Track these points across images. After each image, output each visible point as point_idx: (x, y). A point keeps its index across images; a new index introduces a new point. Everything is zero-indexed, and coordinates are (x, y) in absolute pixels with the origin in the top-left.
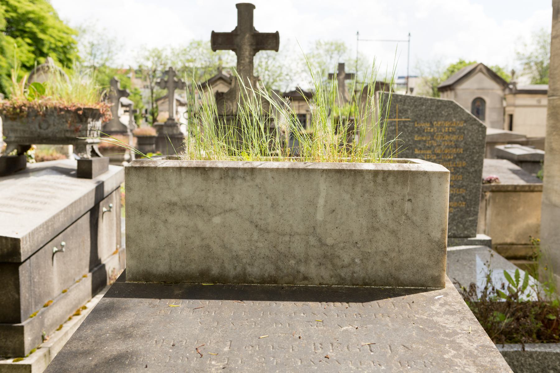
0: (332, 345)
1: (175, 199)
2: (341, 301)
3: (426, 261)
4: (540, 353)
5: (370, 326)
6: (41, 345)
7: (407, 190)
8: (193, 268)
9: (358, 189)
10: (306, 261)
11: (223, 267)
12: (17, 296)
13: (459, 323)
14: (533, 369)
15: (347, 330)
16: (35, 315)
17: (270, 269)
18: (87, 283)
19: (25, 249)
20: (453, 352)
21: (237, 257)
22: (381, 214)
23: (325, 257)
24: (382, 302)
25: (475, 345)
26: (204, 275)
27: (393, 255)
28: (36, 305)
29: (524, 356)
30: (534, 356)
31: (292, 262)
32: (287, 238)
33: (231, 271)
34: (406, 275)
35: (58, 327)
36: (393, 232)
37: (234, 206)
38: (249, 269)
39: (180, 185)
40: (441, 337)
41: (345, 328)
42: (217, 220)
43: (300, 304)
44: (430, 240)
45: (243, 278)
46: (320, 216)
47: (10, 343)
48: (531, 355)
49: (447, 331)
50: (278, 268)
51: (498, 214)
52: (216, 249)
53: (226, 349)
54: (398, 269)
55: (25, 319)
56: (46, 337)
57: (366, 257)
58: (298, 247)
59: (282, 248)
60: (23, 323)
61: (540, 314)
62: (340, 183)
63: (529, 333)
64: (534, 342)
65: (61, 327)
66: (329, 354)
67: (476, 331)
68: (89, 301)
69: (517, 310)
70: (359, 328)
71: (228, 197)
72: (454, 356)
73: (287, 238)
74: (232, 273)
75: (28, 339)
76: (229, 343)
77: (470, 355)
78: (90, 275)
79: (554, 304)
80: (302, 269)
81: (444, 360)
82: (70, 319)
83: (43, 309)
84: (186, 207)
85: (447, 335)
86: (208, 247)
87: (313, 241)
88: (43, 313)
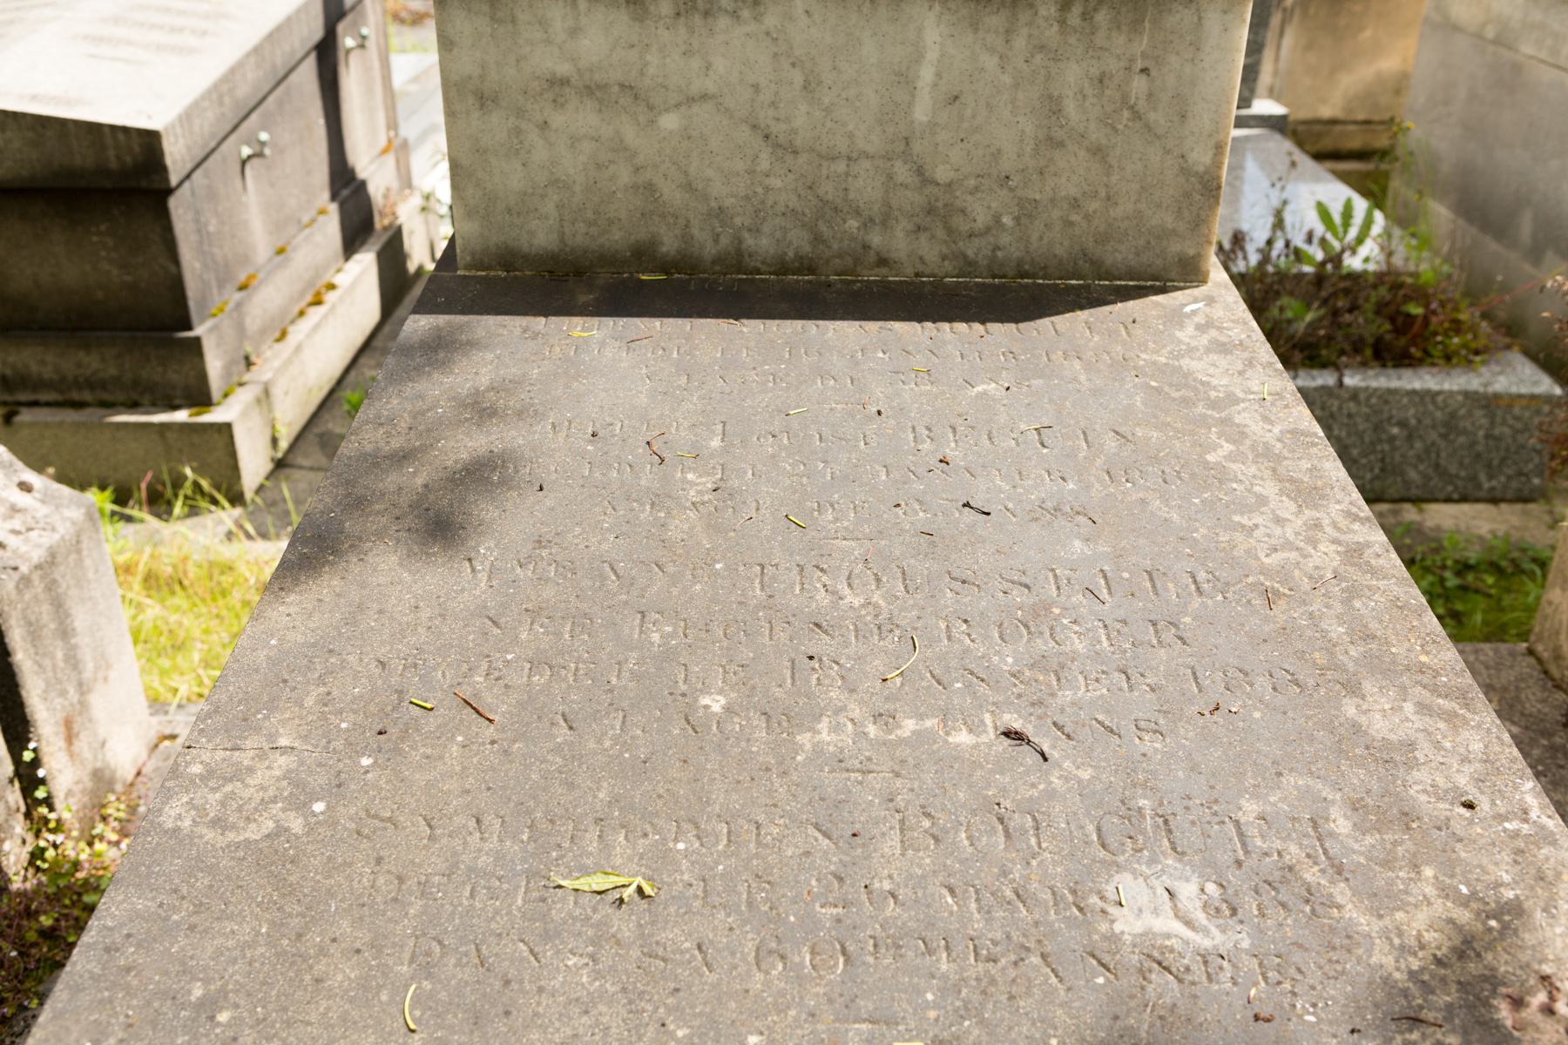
0: (954, 430)
1: (564, 69)
2: (967, 319)
3: (1169, 220)
4: (1376, 390)
5: (1037, 382)
6: (246, 377)
7: (1143, 43)
8: (617, 239)
9: (1020, 42)
10: (886, 220)
11: (686, 237)
12: (173, 269)
13: (1241, 373)
14: (1355, 425)
15: (985, 393)
16: (222, 310)
17: (798, 241)
18: (331, 228)
19: (176, 155)
20: (1228, 447)
21: (720, 213)
22: (1070, 107)
23: (930, 211)
24: (1063, 321)
25: (1276, 430)
26: (643, 254)
27: (1093, 206)
28: (221, 286)
29: (1338, 397)
30: (1362, 396)
31: (853, 224)
32: (841, 167)
33: (707, 243)
34: (1119, 254)
35: (277, 334)
36: (1098, 152)
37: (710, 85)
38: (749, 241)
39: (574, 32)
40: (1200, 409)
41: (980, 388)
42: (670, 122)
43: (873, 326)
44: (1185, 171)
45: (736, 261)
46: (921, 113)
47: (176, 375)
48: (1355, 394)
49: (1213, 394)
50: (817, 239)
51: (1309, 47)
52: (671, 193)
53: (716, 443)
54: (1102, 239)
55: (203, 320)
56: (253, 358)
57: (1027, 211)
58: (866, 188)
59: (828, 189)
60: (198, 331)
61: (1387, 304)
62: (975, 27)
63: (1357, 347)
64: (1364, 364)
65: (283, 335)
66: (950, 454)
67: (1279, 395)
68: (339, 271)
69: (1334, 295)
70: (1013, 389)
71: (696, 63)
72: (1229, 457)
73: (841, 167)
74: (710, 250)
75: (214, 365)
76: (720, 427)
77: (1264, 453)
78: (333, 208)
79: (1422, 280)
80: (876, 239)
81: (1207, 466)
82: (302, 313)
83: (238, 296)
84: (593, 91)
85: (1214, 405)
86: (650, 187)
87: (902, 172)
88: (239, 305)
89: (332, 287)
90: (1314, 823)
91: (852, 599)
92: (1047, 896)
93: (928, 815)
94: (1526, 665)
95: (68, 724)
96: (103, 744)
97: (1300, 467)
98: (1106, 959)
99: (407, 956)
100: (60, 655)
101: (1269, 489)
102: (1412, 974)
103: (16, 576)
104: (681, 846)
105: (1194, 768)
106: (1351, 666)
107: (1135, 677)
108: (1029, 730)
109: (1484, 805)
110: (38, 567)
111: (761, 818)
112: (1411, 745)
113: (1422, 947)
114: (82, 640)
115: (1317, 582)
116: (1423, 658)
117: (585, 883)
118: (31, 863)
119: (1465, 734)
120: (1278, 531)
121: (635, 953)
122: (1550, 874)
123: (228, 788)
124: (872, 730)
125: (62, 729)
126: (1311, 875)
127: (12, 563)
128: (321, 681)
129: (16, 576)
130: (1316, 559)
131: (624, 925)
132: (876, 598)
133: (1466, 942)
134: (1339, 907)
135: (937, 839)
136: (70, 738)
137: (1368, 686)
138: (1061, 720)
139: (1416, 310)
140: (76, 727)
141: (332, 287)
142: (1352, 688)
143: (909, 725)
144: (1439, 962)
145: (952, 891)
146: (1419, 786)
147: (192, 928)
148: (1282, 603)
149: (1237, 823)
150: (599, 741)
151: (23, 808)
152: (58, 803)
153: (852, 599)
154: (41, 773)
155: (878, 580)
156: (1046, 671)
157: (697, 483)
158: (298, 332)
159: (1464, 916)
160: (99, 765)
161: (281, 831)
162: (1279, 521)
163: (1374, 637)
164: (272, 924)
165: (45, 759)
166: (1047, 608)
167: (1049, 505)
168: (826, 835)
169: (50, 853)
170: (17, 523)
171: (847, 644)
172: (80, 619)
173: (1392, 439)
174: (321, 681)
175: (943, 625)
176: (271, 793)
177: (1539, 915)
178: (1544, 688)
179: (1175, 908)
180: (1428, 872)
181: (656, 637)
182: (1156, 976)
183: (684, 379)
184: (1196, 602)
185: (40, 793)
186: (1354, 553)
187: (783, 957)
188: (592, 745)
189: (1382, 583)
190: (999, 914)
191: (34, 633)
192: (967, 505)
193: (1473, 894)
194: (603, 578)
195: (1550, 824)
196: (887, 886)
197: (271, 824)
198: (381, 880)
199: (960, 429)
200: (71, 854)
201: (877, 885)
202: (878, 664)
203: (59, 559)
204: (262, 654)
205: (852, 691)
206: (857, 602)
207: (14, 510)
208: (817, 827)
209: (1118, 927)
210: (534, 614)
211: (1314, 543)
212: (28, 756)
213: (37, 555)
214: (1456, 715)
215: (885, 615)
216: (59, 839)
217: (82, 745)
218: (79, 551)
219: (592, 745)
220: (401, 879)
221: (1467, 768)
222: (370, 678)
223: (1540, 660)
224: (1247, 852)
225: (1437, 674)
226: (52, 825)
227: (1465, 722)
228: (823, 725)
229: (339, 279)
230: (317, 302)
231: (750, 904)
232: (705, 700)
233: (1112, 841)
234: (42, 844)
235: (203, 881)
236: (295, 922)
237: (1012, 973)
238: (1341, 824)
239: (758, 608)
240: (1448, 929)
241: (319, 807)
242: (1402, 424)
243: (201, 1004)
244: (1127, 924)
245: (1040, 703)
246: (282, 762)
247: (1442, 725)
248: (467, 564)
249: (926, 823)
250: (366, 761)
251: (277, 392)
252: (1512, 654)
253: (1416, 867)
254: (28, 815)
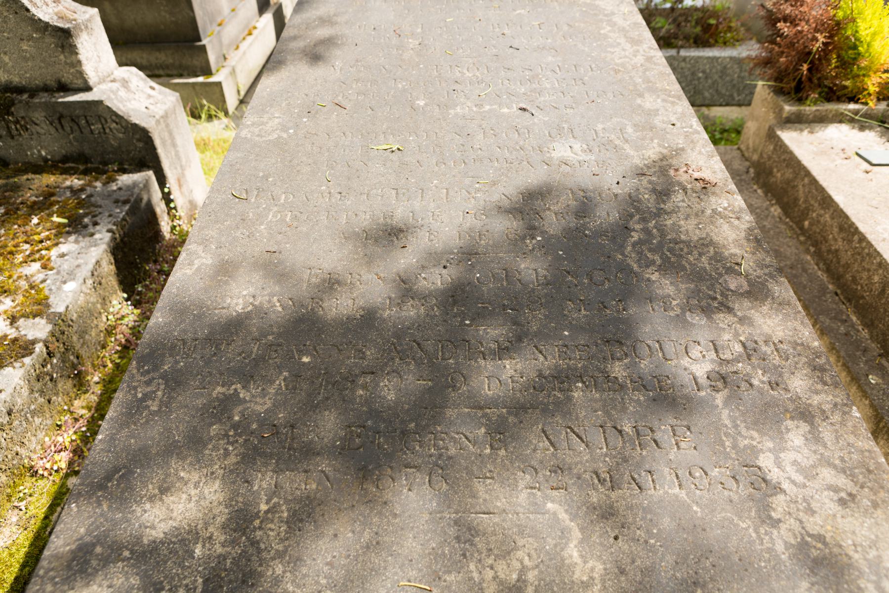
0: (508, 25)
4: (693, 57)
5: (540, 10)
6: (225, 64)
12: (191, 14)
13: (618, 5)
14: (684, 73)
15: (520, 14)
16: (212, 34)
20: (609, 28)
25: (628, 23)
28: (211, 23)
29: (677, 60)
30: (688, 60)
35: (235, 47)
40: (601, 17)
41: (518, 12)
47: (197, 62)
48: (684, 59)
49: (606, 12)
53: (419, 30)
55: (205, 38)
56: (227, 56)
60: (204, 42)
61: (702, 18)
63: (686, 38)
64: (690, 47)
65: (237, 48)
66: (505, 32)
67: (631, 12)
68: (257, 21)
69: (680, 15)
70: (531, 12)
72: (609, 31)
76: (420, 26)
77: (623, 30)
79: (716, 8)
81: (600, 34)
82: (244, 39)
83: (218, 28)
85: (606, 15)
88: (219, 32)
89: (255, 28)
90: (621, 130)
91: (468, 74)
92: (531, 148)
93: (492, 130)
94: (736, 153)
95: (179, 181)
96: (192, 191)
97: (635, 34)
98: (548, 162)
99: (325, 165)
100: (173, 153)
101: (622, 40)
102: (645, 165)
103: (155, 119)
104: (411, 138)
105: (583, 117)
106: (642, 90)
107: (566, 94)
108: (528, 108)
109: (678, 125)
110: (162, 117)
111: (437, 131)
112: (658, 110)
113: (649, 158)
114: (180, 149)
115: (634, 67)
116: (668, 87)
117: (380, 147)
118: (172, 232)
119: (677, 107)
120: (623, 53)
121: (398, 163)
122: (695, 141)
123: (261, 127)
124: (475, 109)
125: (177, 182)
126: (617, 142)
127: (153, 115)
128: (286, 99)
129: (155, 119)
130: (635, 60)
131: (394, 157)
132: (478, 74)
133: (664, 157)
134: (625, 150)
135: (495, 136)
136: (180, 186)
137: (646, 95)
138: (539, 105)
139: (713, 21)
140: (182, 183)
141: (255, 28)
142: (641, 95)
143: (487, 108)
144: (654, 162)
145: (499, 148)
146: (657, 121)
147: (256, 160)
148: (621, 73)
149: (595, 131)
150: (383, 113)
151: (166, 211)
152: (179, 209)
153: (468, 74)
154: (172, 197)
155: (478, 69)
156: (535, 93)
157: (412, 43)
158: (244, 46)
159: (665, 151)
160: (191, 198)
161: (279, 137)
162: (624, 50)
163: (651, 82)
164: (281, 159)
165: (173, 192)
166: (537, 75)
167: (541, 46)
168: (459, 135)
169: (178, 228)
170: (151, 101)
171: (466, 87)
172: (179, 141)
173: (699, 79)
174: (286, 99)
175: (500, 81)
176: (275, 128)
177: (689, 151)
178: (741, 160)
179: (572, 151)
180: (656, 141)
181: (400, 86)
182: (563, 166)
183: (406, 11)
184: (590, 73)
185: (172, 205)
186: (649, 59)
187: (445, 164)
188: (380, 114)
189: (657, 67)
190: (514, 153)
191: (164, 143)
192: (511, 47)
193: (669, 146)
194: (381, 70)
195: (699, 129)
196: (478, 147)
197: (277, 136)
198: (314, 148)
199: (510, 25)
200: (186, 229)
201: (475, 146)
202: (477, 92)
203: (169, 115)
204: (265, 93)
205: (468, 99)
206: (470, 75)
207: (150, 96)
208: (456, 133)
209: (552, 155)
210: (357, 81)
211: (635, 56)
212: (166, 190)
213: (161, 113)
214: (675, 102)
215: (480, 78)
216: (181, 223)
217: (184, 189)
218: (175, 114)
219: (380, 114)
220: (321, 148)
221: (675, 116)
222: (303, 99)
223: (741, 151)
224: (597, 137)
225: (671, 91)
226: (178, 217)
227: (678, 104)
228: (458, 108)
229: (258, 25)
230: (250, 34)
231: (434, 151)
232: (418, 102)
233: (553, 135)
234: (175, 224)
235: (257, 149)
236: (289, 158)
237: (518, 166)
238: (630, 130)
239: (435, 77)
240: (660, 155)
241: (291, 131)
242: (704, 72)
243: (263, 177)
244: (556, 155)
245: (533, 101)
246: (277, 121)
247: (669, 105)
248: (332, 68)
249: (492, 132)
250: (305, 120)
251: (238, 71)
252: (731, 150)
253: (652, 140)
254: (168, 214)
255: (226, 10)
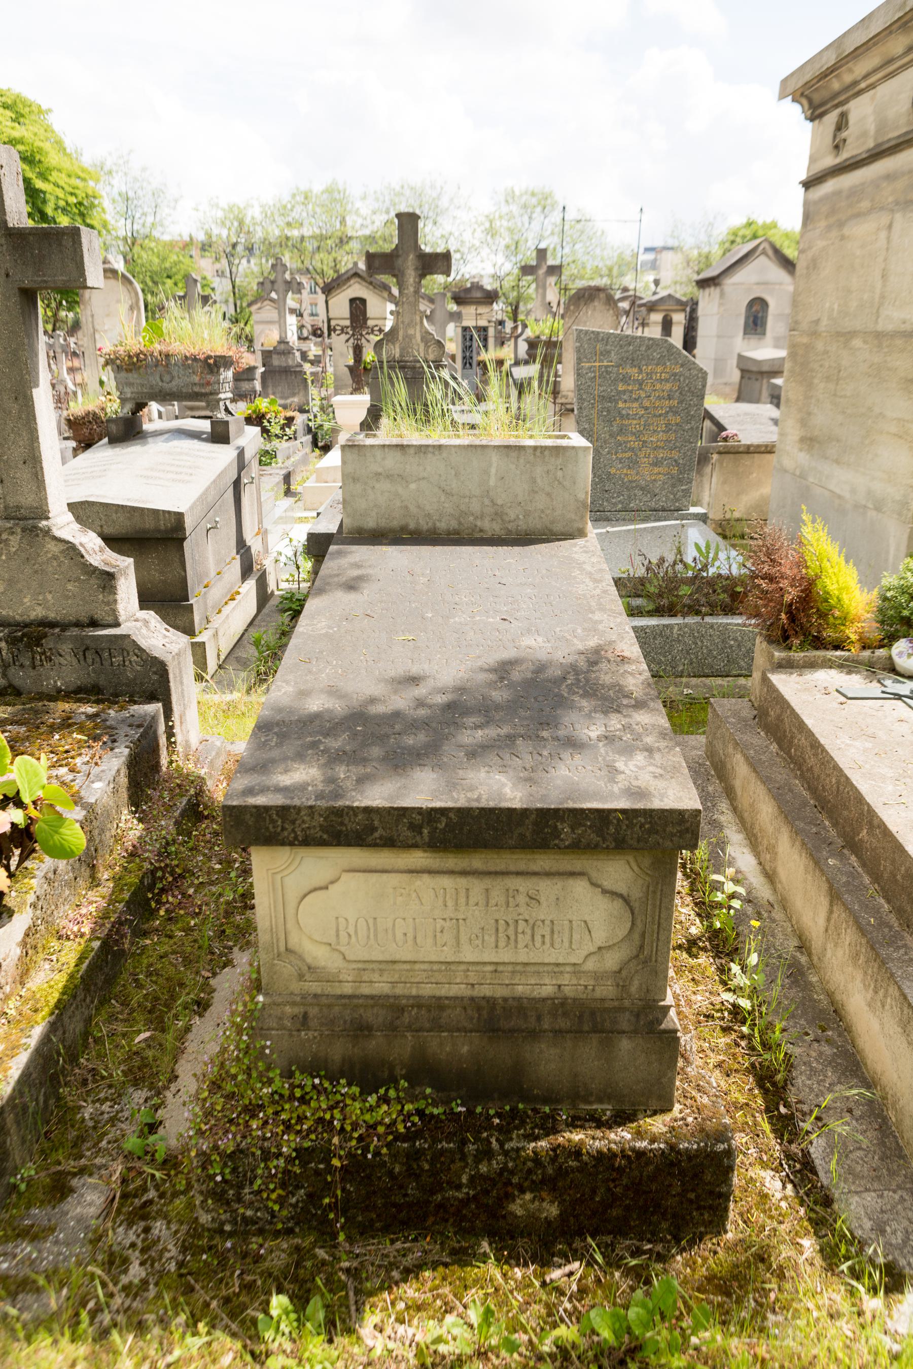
1: (380, 470)
2: (507, 545)
3: (573, 517)
7: (560, 461)
8: (395, 524)
9: (522, 461)
10: (482, 517)
11: (418, 523)
17: (454, 524)
18: (236, 567)
19: (189, 523)
21: (429, 515)
22: (539, 480)
23: (496, 514)
24: (537, 546)
26: (404, 529)
27: (548, 512)
31: (471, 518)
32: (467, 500)
33: (424, 526)
34: (558, 527)
36: (548, 494)
37: (425, 475)
38: (438, 524)
39: (383, 459)
42: (413, 486)
43: (477, 548)
44: (577, 500)
46: (492, 482)
50: (460, 523)
51: (725, 482)
52: (413, 509)
54: (552, 522)
57: (527, 514)
58: (475, 507)
59: (463, 507)
62: (508, 456)
65: (220, 612)
71: (421, 468)
73: (467, 500)
74: (425, 527)
75: (197, 618)
77: (590, 574)
78: (238, 557)
80: (479, 523)
84: (389, 477)
86: (406, 507)
87: (487, 501)
89: (238, 593)
101: (587, 580)
131: (411, 643)
139: (739, 589)
141: (238, 593)
146: (600, 627)
157: (423, 580)
158: (227, 610)
173: (731, 647)
207: (165, 636)
213: (176, 651)
229: (240, 590)
230: (233, 599)
238: (579, 631)
242: (735, 640)
251: (220, 633)
255: (213, 573)
